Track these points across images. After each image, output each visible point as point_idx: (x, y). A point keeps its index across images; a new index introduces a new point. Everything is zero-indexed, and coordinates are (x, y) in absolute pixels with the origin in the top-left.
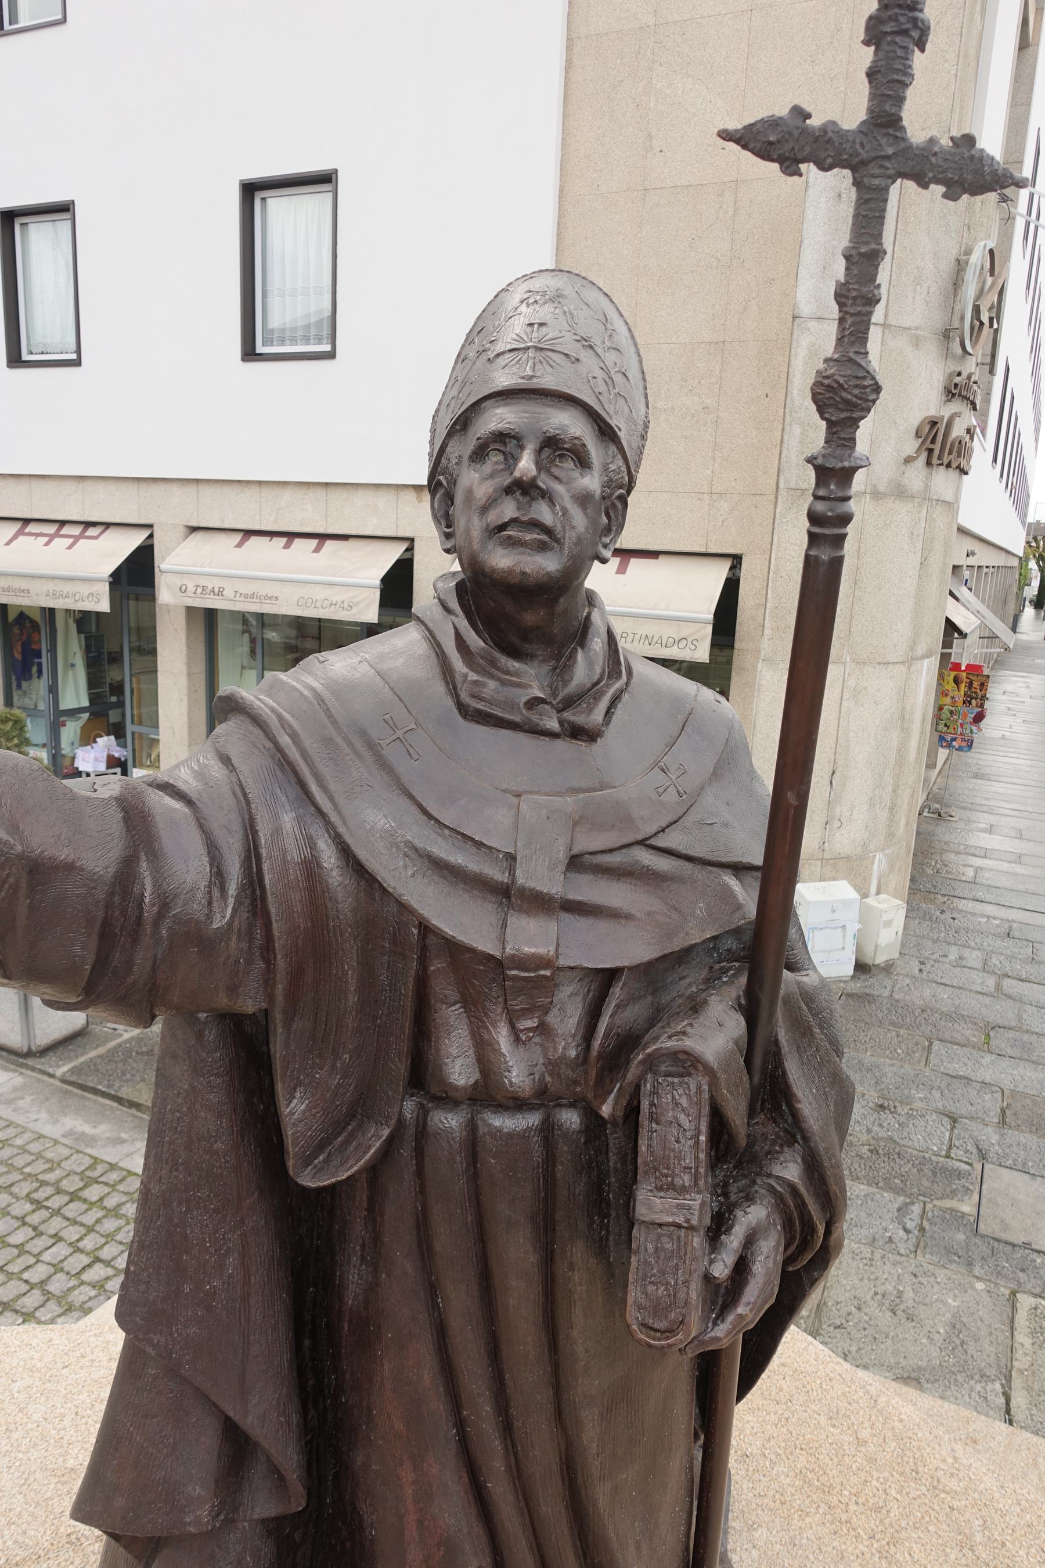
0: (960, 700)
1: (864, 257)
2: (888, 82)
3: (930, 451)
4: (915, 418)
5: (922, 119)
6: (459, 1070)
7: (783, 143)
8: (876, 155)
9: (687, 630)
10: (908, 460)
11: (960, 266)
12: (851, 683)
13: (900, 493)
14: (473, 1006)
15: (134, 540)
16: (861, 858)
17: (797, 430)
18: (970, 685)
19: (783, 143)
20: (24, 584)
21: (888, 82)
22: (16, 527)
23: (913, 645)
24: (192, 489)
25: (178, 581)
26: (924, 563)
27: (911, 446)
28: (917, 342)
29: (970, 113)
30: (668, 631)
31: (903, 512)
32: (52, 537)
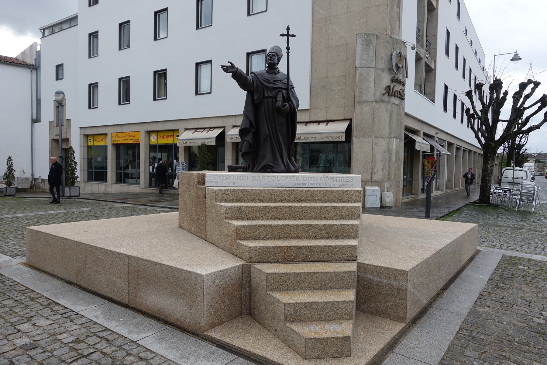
0: (430, 167)
1: (288, 41)
2: (288, 32)
3: (389, 93)
4: (385, 86)
5: (290, 33)
6: (266, 95)
7: (282, 35)
8: (288, 35)
9: (340, 135)
10: (384, 94)
11: (392, 55)
12: (375, 142)
13: (382, 101)
14: (267, 91)
15: (221, 130)
16: (382, 182)
17: (358, 89)
18: (432, 163)
19: (282, 35)
20: (196, 141)
21: (288, 32)
22: (194, 131)
23: (390, 134)
24: (234, 117)
25: (231, 137)
26: (390, 116)
27: (384, 92)
28: (383, 71)
29: (397, 27)
30: (336, 135)
31: (384, 106)
32: (202, 132)
